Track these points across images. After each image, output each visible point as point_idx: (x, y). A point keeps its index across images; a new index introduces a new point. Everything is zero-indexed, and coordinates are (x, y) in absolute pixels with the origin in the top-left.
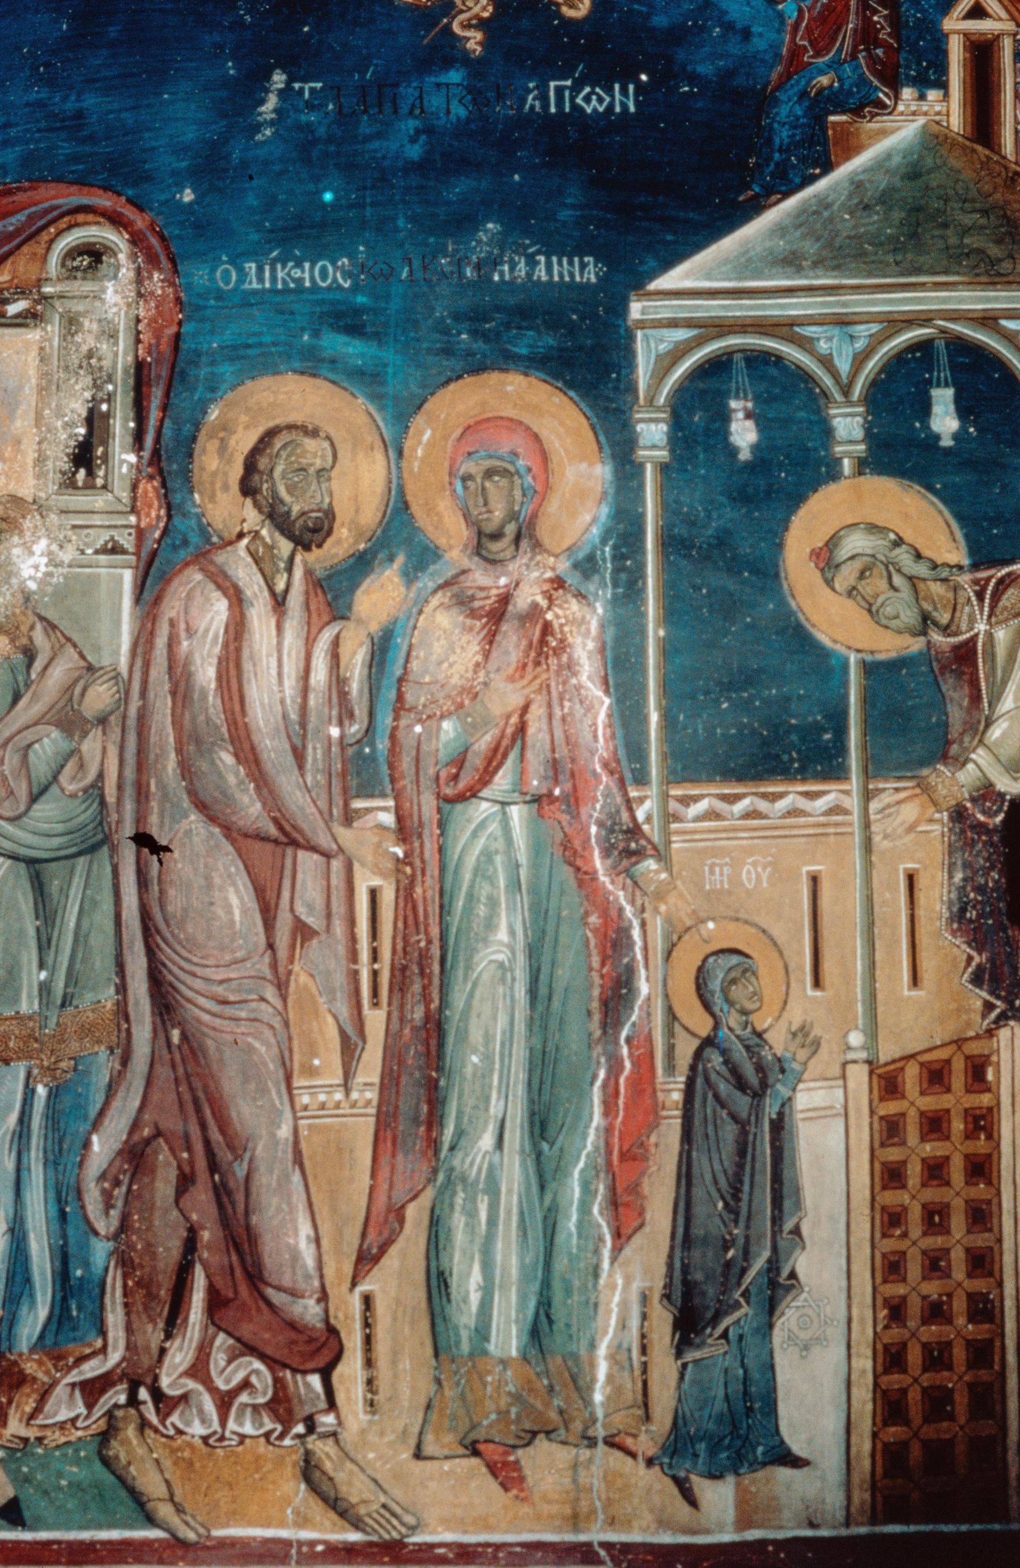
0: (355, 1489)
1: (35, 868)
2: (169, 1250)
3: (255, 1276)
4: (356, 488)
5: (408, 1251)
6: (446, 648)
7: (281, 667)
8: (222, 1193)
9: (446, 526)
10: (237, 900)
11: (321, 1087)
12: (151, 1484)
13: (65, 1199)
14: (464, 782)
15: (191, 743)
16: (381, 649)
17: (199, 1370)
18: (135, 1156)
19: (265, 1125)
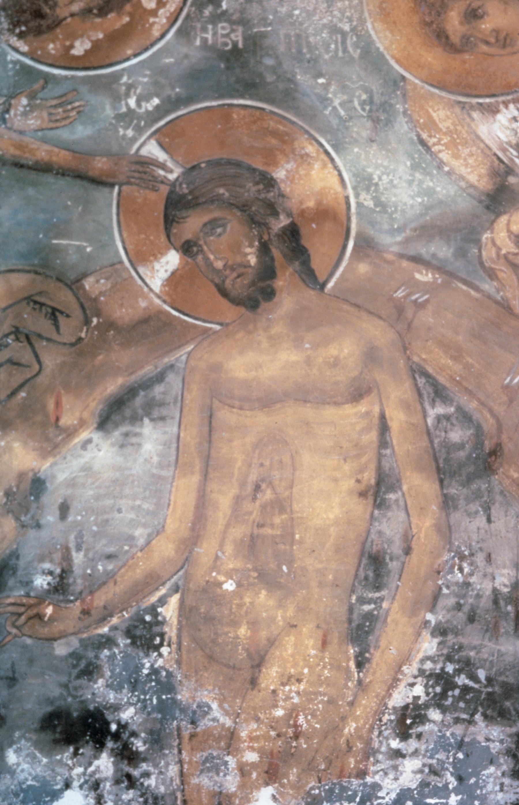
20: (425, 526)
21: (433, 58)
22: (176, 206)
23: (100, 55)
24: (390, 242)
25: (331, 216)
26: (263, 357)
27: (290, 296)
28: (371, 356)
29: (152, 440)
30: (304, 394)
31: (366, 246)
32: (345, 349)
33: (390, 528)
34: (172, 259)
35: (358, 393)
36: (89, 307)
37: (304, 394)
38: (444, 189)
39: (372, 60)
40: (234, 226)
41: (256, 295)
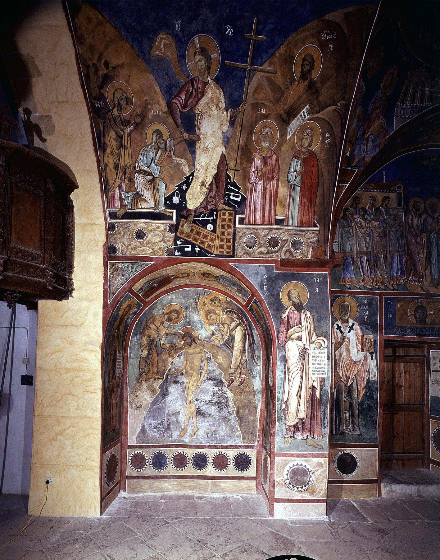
0: (425, 289)
1: (397, 238)
2: (410, 269)
3: (417, 271)
4: (422, 206)
5: (429, 269)
6: (429, 220)
7: (416, 222)
8: (414, 264)
9: (429, 210)
10: (413, 241)
11: (421, 256)
12: (408, 287)
13: (401, 264)
14: (431, 231)
15: (410, 227)
16: (424, 220)
17: (412, 278)
18: (406, 261)
19: (417, 258)
20: (206, 364)
21: (207, 321)
22: (184, 336)
23: (176, 323)
24: (203, 339)
25: (198, 337)
26: (191, 350)
27: (194, 345)
28: (201, 350)
29: (182, 357)
30: (195, 353)
31: (200, 340)
32: (199, 349)
33: (203, 365)
34: (183, 342)
35: (200, 353)
36: (176, 346)
37: (195, 353)
38: (208, 334)
39: (201, 322)
40: (189, 338)
41: (191, 345)
